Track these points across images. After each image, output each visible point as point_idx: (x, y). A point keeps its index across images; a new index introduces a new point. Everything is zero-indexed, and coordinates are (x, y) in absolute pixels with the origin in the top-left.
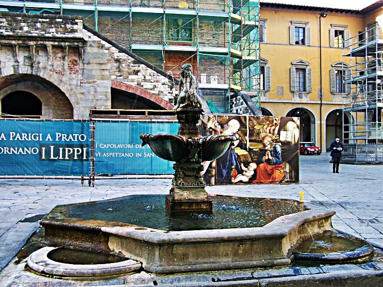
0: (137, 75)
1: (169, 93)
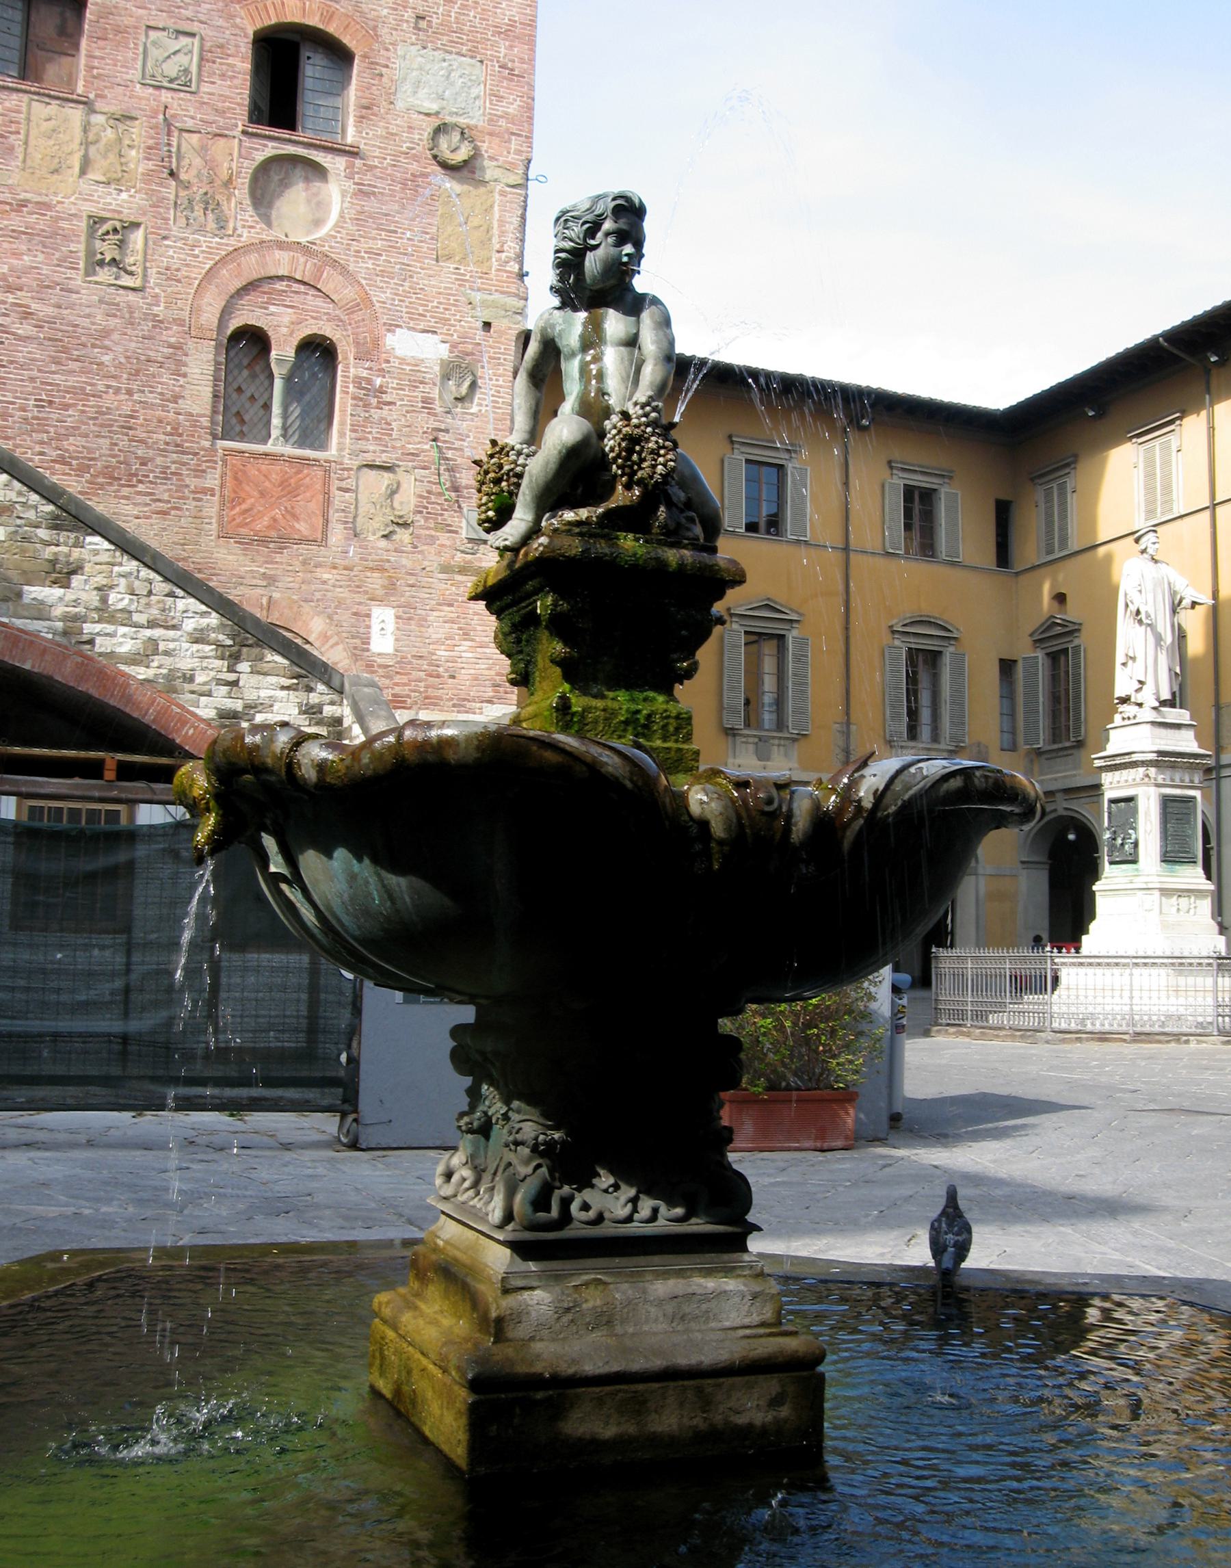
0: (67, 586)
1: (220, 682)
